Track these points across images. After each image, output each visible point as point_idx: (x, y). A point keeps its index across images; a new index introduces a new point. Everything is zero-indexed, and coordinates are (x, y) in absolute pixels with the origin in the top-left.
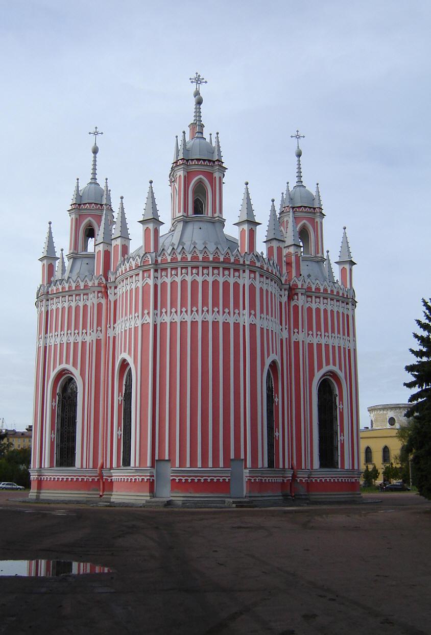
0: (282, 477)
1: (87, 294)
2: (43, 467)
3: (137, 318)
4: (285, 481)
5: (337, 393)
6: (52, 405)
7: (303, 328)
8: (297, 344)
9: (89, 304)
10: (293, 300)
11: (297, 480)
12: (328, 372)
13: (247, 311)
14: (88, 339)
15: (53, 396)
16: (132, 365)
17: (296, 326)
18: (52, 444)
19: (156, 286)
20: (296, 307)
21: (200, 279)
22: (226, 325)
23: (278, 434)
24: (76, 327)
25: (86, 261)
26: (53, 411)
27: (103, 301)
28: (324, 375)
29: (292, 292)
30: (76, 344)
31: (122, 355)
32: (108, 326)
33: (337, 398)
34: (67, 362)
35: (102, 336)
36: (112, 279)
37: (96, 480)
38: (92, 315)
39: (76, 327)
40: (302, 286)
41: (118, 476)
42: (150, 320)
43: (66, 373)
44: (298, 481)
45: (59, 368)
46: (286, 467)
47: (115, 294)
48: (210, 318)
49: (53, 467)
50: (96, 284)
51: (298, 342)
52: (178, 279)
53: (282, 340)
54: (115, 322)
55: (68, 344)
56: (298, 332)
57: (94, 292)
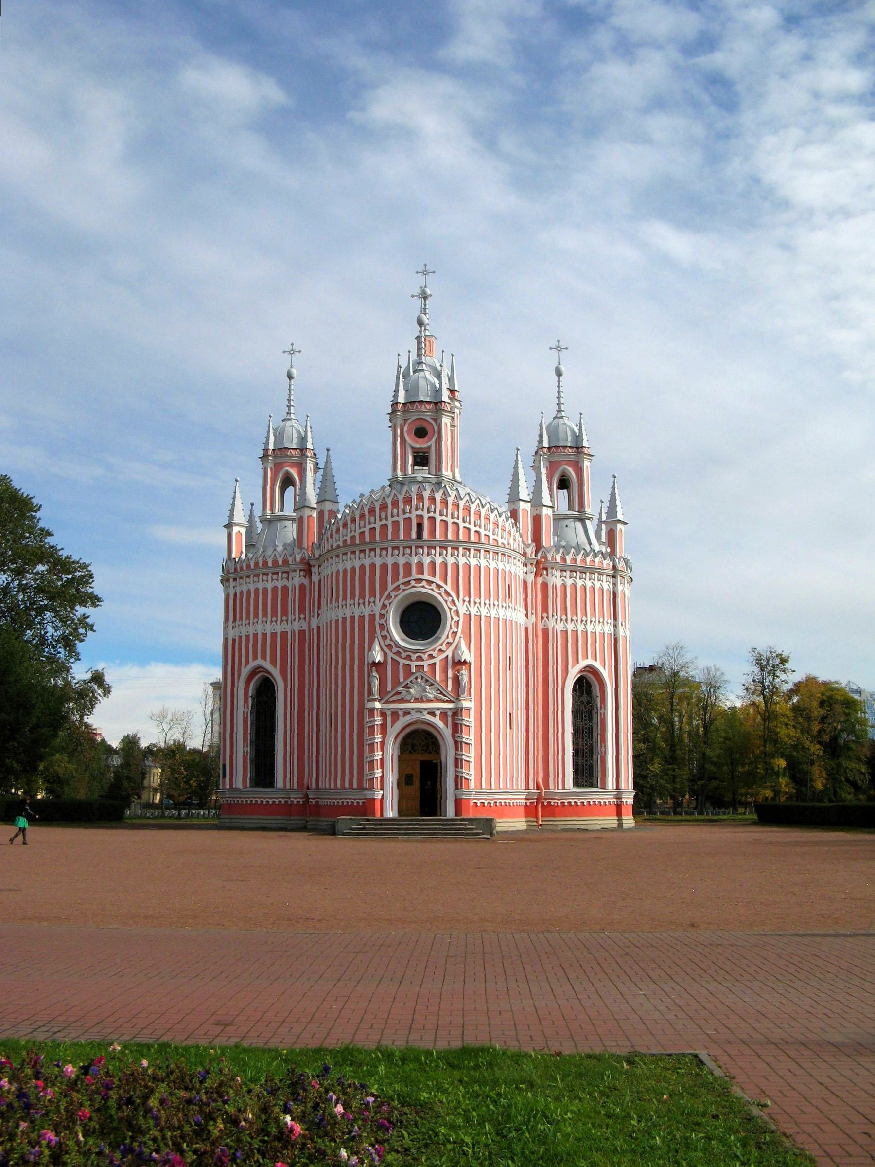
0: (526, 799)
1: (288, 573)
2: (234, 786)
3: (344, 607)
4: (528, 804)
5: (599, 695)
6: (244, 712)
7: (553, 612)
8: (545, 632)
10: (541, 575)
11: (543, 802)
12: (585, 667)
17: (545, 609)
18: (245, 758)
20: (545, 585)
24: (274, 613)
26: (245, 719)
27: (306, 582)
28: (581, 671)
29: (541, 567)
30: (274, 635)
32: (312, 614)
33: (599, 699)
34: (264, 657)
36: (317, 556)
37: (301, 803)
38: (294, 600)
39: (274, 613)
40: (552, 560)
41: (326, 799)
43: (260, 672)
44: (546, 804)
45: (253, 664)
46: (531, 786)
47: (319, 573)
49: (247, 787)
50: (298, 560)
51: (547, 629)
53: (526, 629)
54: (319, 608)
55: (264, 635)
56: (548, 618)
57: (295, 571)
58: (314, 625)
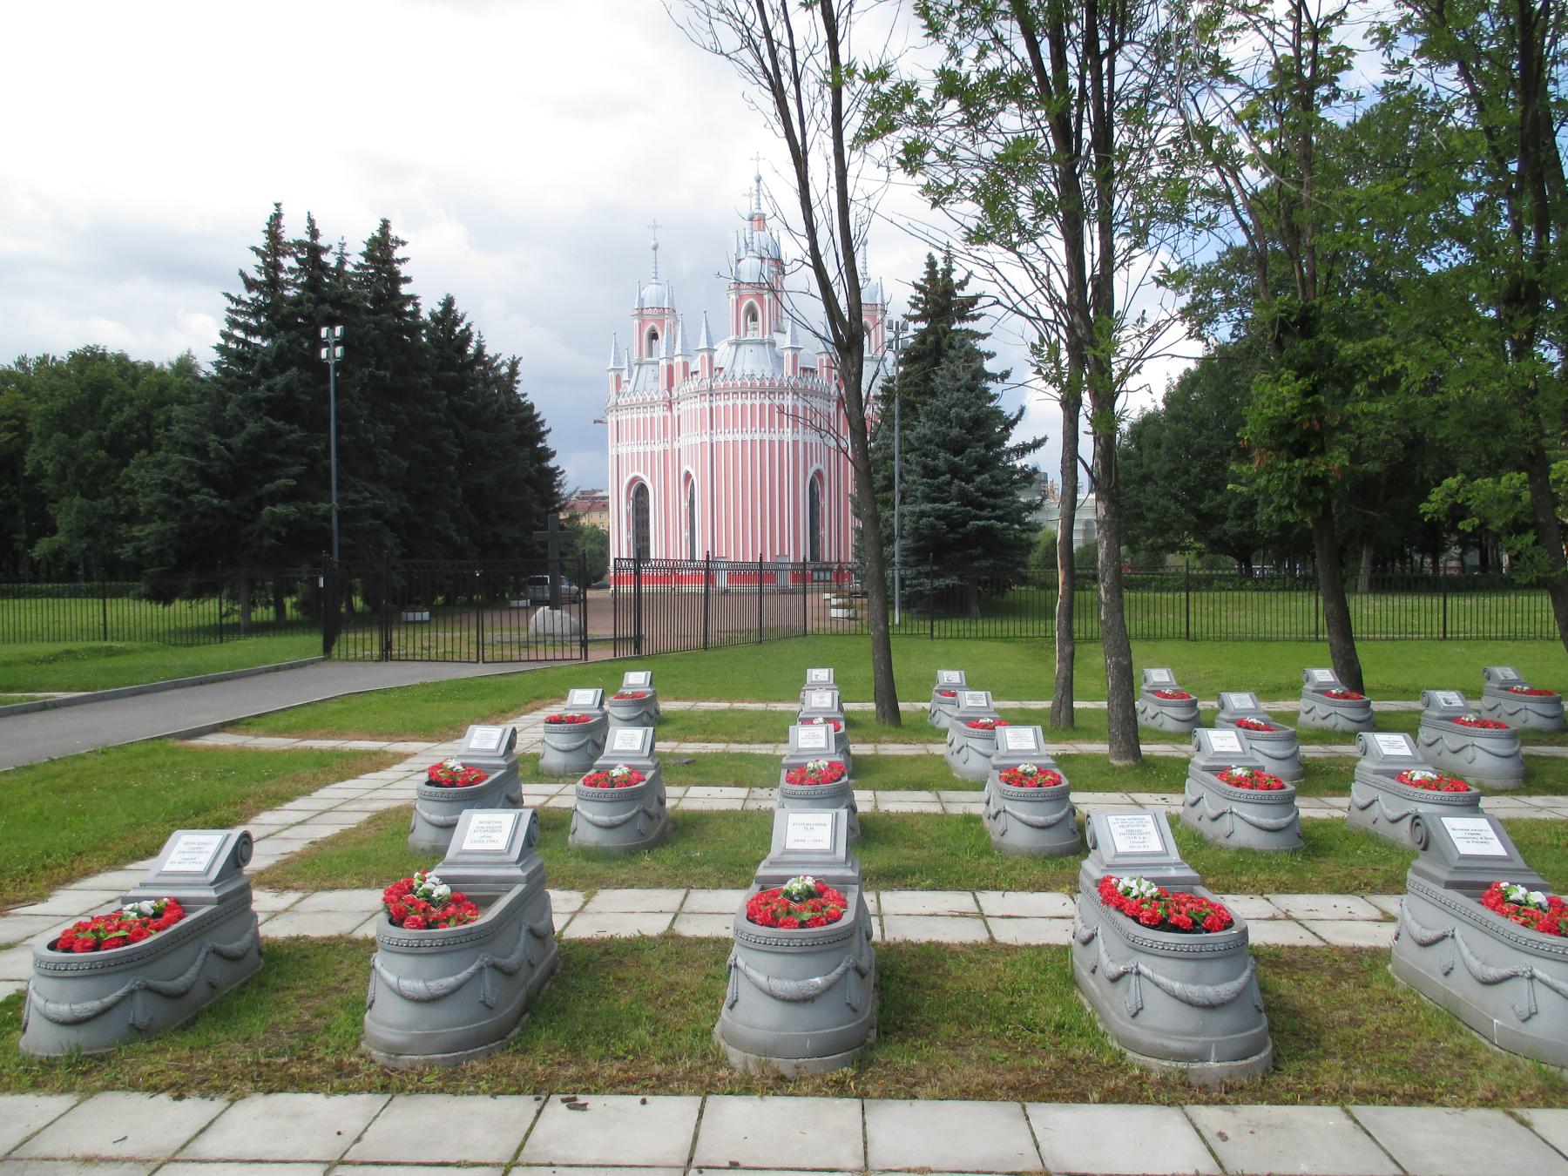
9: (655, 415)
13: (790, 430)
14: (656, 448)
15: (627, 502)
16: (694, 477)
19: (711, 409)
21: (748, 402)
22: (771, 442)
23: (824, 532)
25: (651, 367)
27: (668, 414)
31: (685, 467)
34: (639, 470)
35: (668, 447)
42: (707, 439)
45: (631, 476)
48: (757, 437)
52: (730, 403)
58: (676, 446)
